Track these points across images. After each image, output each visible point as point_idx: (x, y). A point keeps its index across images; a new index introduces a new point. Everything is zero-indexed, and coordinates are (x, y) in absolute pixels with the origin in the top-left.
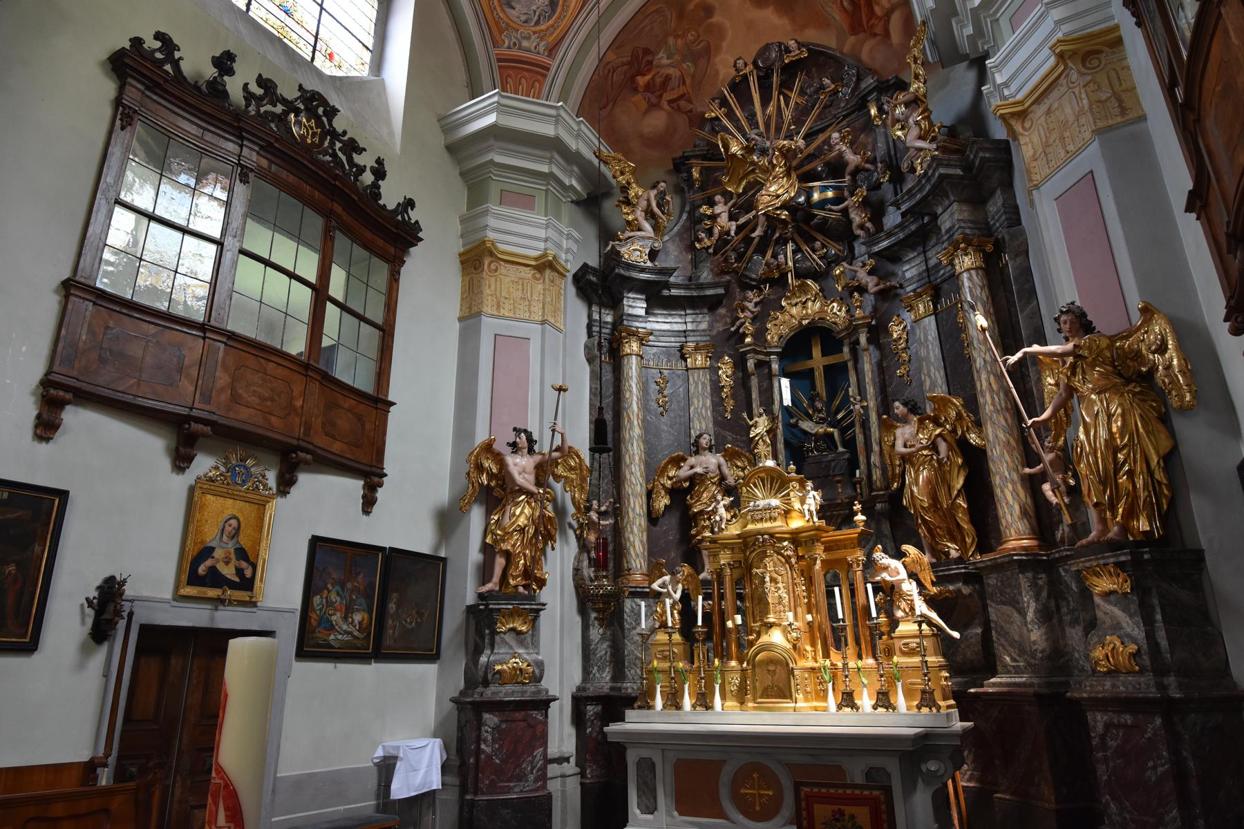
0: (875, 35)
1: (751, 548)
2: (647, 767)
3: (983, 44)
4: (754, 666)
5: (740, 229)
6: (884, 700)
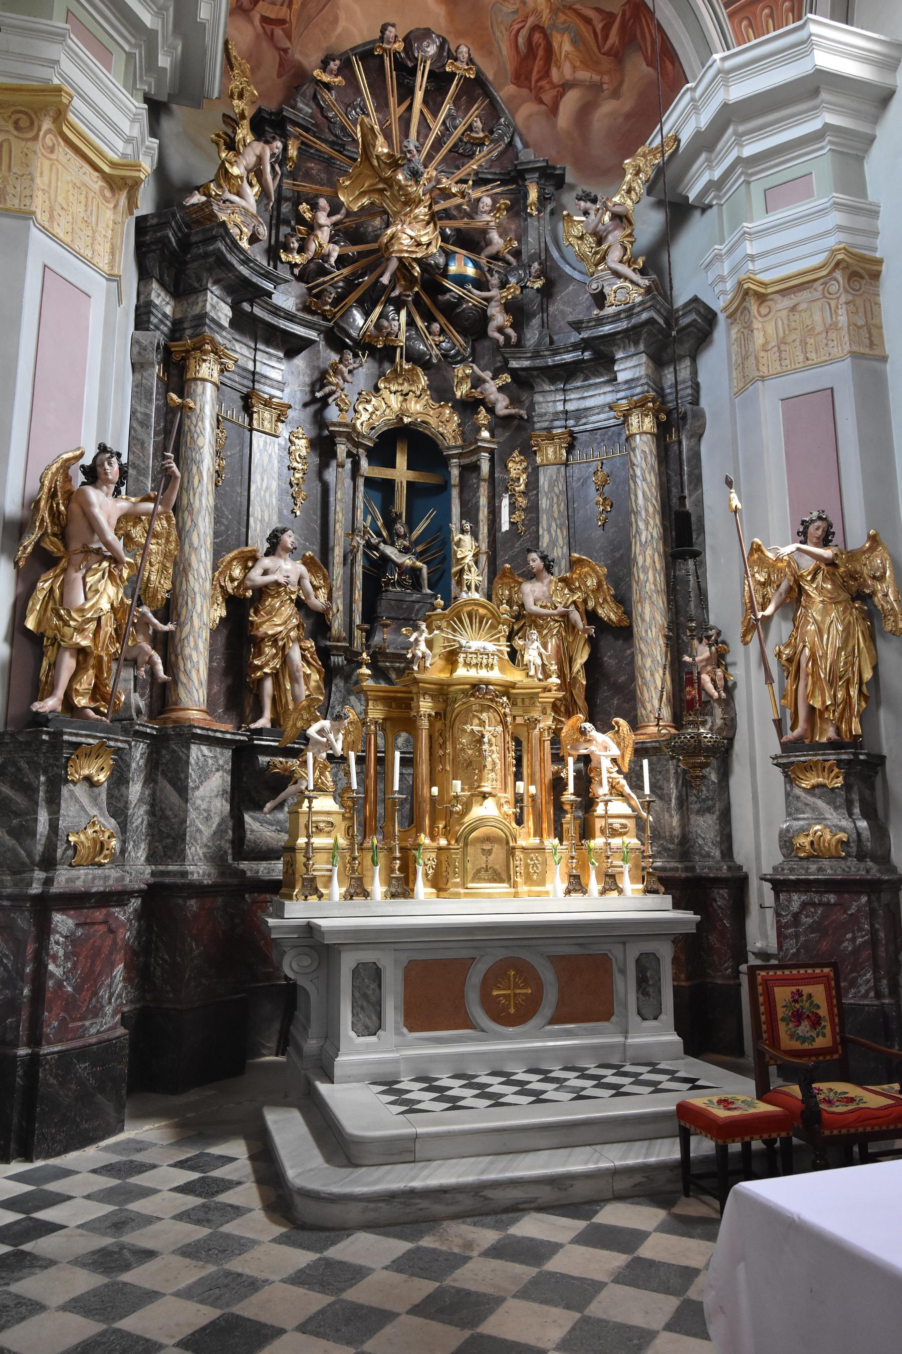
0: (541, 101)
2: (369, 978)
3: (715, 197)
4: (466, 844)
5: (342, 261)
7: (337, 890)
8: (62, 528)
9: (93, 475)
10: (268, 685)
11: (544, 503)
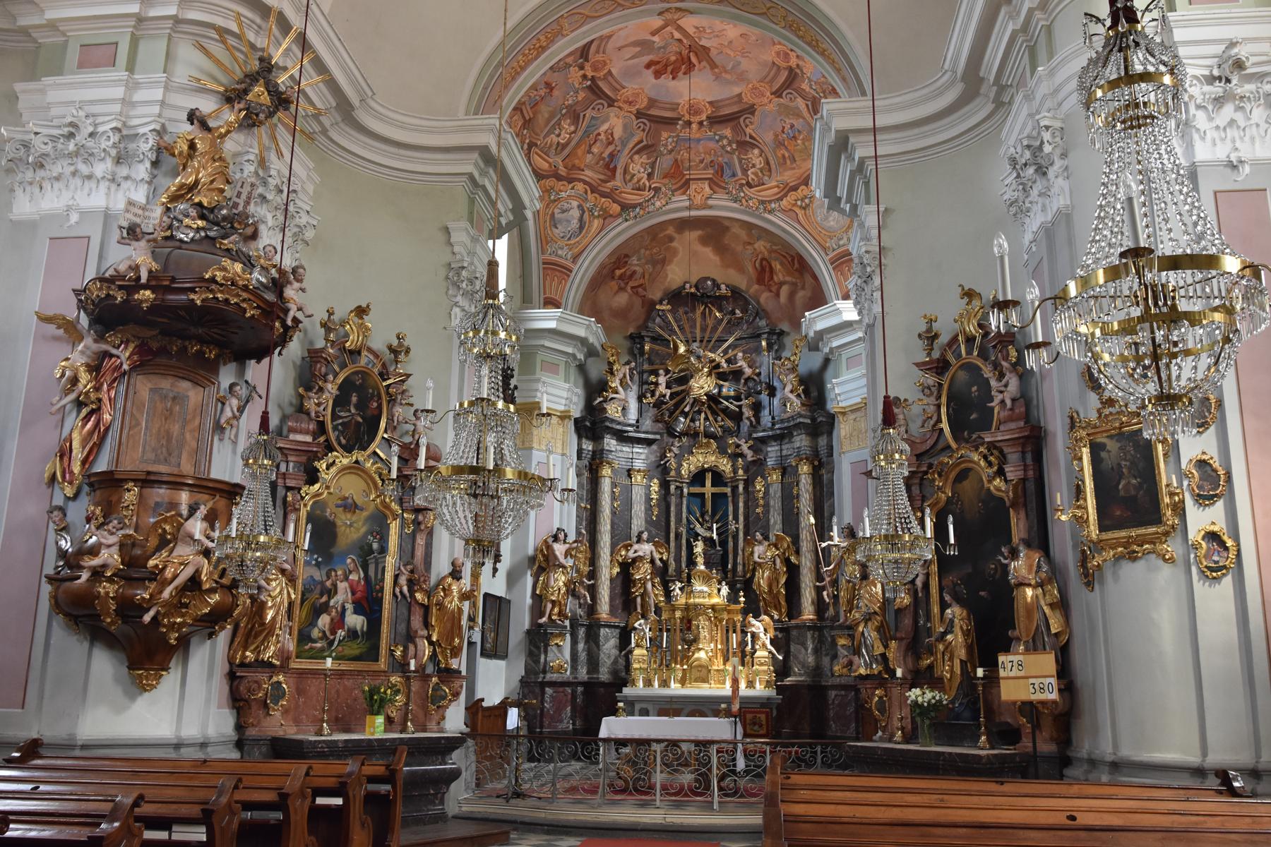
1: (691, 613)
6: (751, 684)
7: (641, 684)
8: (546, 558)
9: (556, 538)
10: (639, 600)
11: (772, 503)
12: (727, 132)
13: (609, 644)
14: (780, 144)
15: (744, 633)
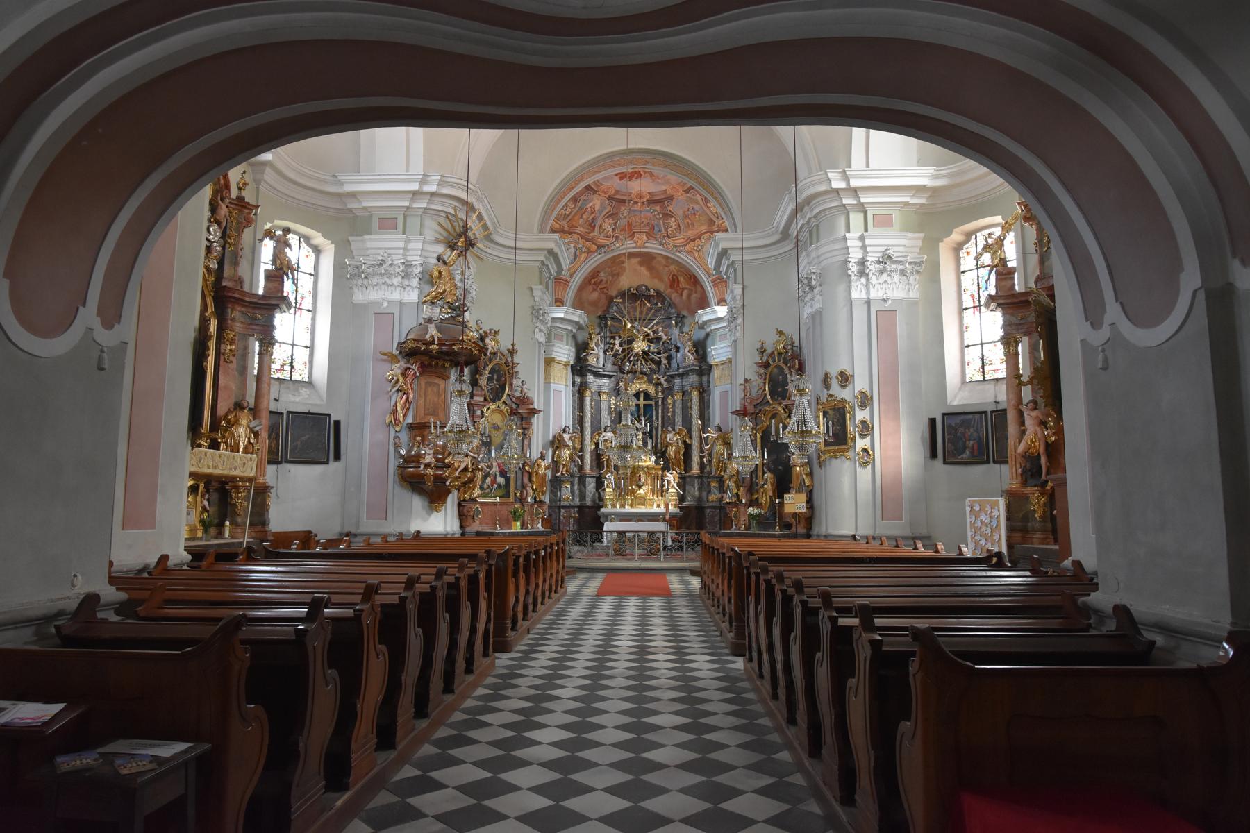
5: (623, 351)
9: (564, 431)
12: (658, 208)
13: (591, 485)
14: (686, 217)
15: (663, 480)
